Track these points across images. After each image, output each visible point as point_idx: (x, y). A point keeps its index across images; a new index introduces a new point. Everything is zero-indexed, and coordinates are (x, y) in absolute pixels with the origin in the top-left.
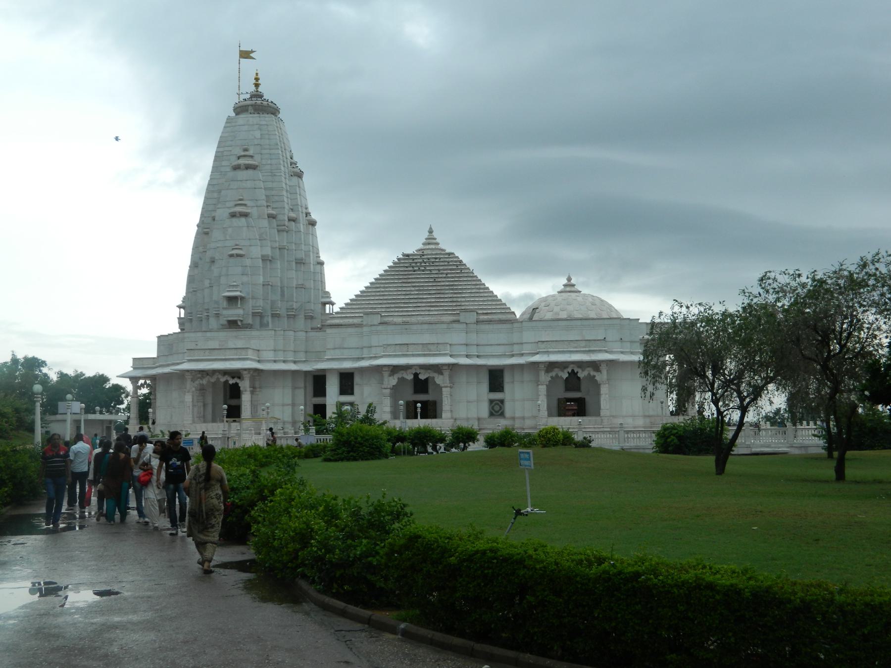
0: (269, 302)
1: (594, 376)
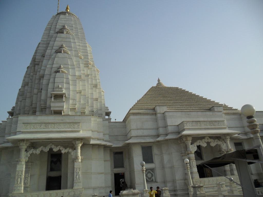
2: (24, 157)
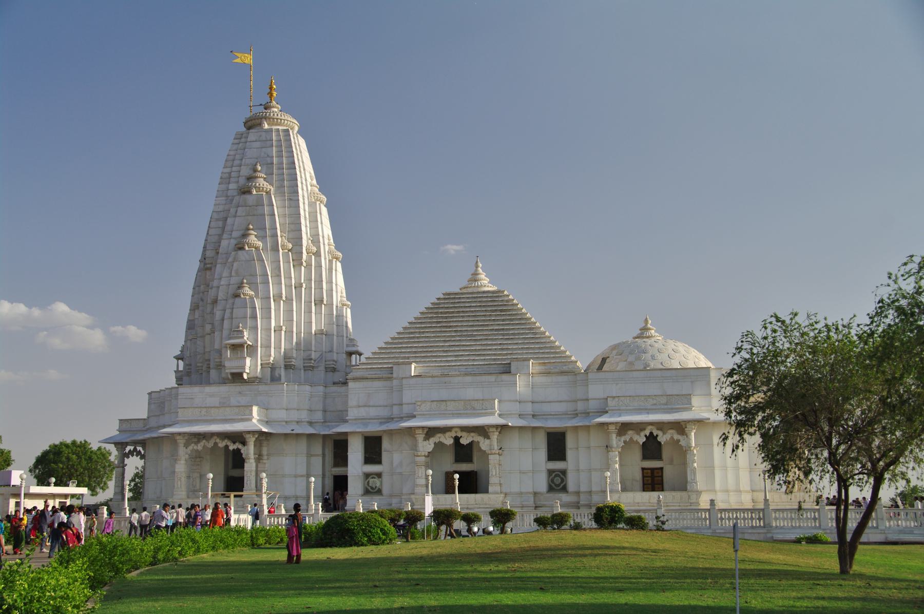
1: (678, 441)
2: (183, 453)
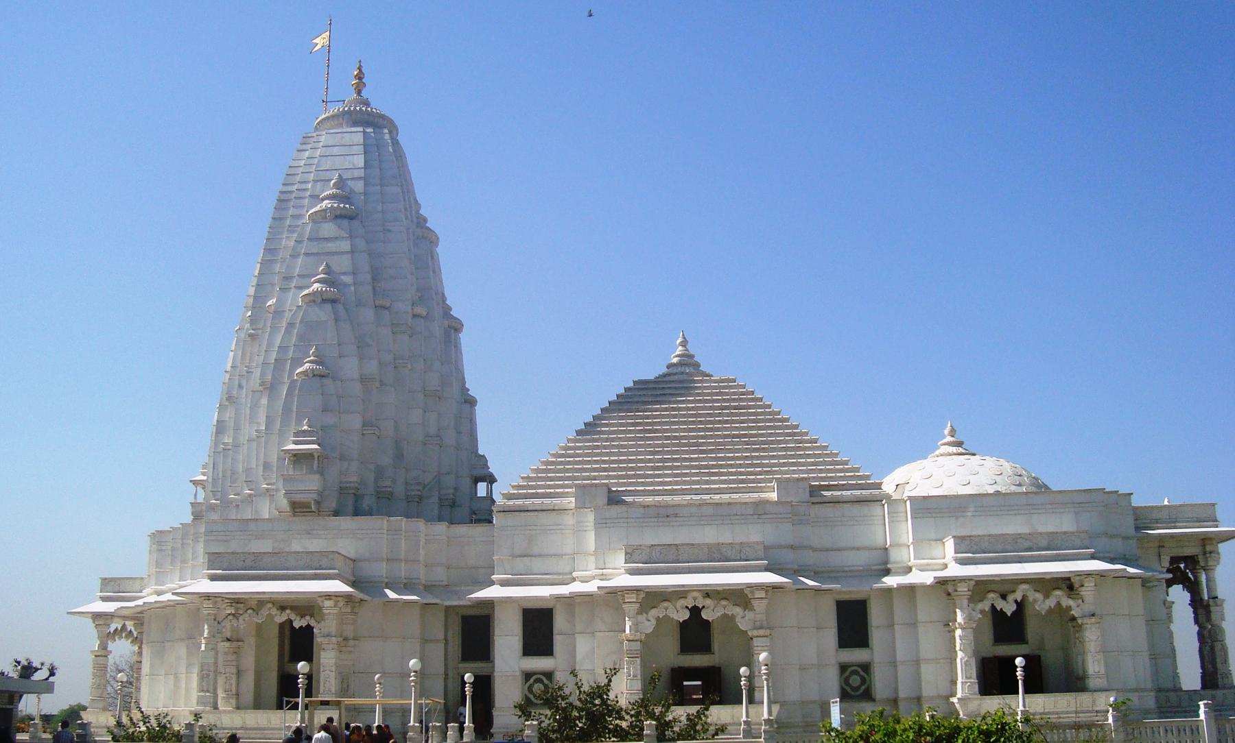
0: (372, 467)
